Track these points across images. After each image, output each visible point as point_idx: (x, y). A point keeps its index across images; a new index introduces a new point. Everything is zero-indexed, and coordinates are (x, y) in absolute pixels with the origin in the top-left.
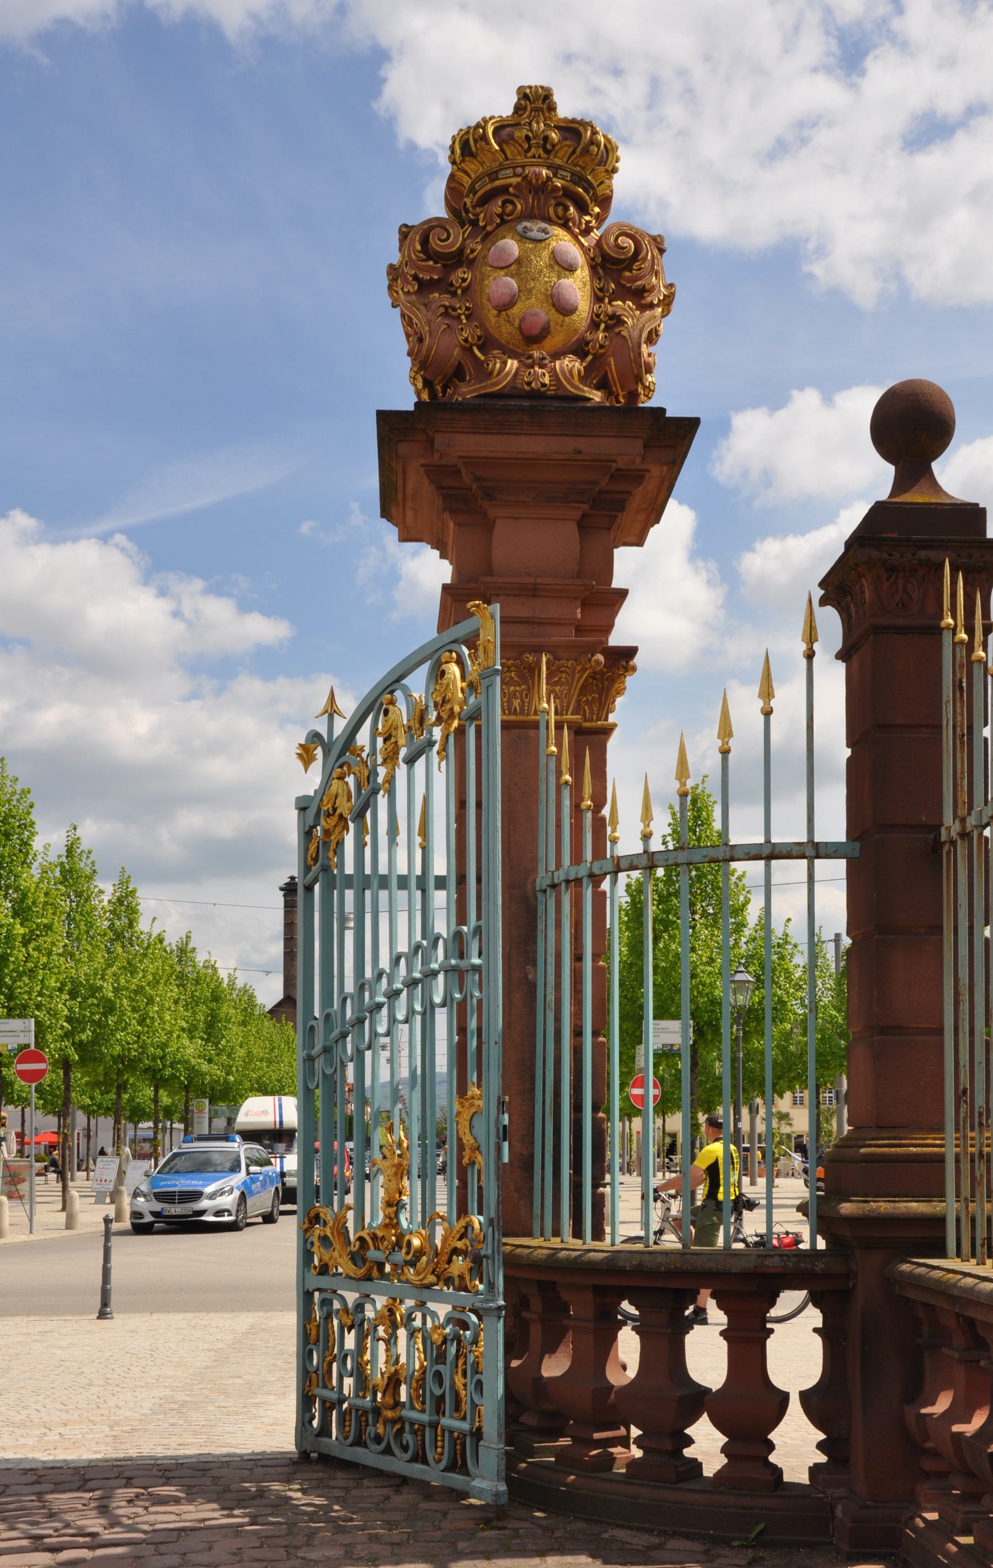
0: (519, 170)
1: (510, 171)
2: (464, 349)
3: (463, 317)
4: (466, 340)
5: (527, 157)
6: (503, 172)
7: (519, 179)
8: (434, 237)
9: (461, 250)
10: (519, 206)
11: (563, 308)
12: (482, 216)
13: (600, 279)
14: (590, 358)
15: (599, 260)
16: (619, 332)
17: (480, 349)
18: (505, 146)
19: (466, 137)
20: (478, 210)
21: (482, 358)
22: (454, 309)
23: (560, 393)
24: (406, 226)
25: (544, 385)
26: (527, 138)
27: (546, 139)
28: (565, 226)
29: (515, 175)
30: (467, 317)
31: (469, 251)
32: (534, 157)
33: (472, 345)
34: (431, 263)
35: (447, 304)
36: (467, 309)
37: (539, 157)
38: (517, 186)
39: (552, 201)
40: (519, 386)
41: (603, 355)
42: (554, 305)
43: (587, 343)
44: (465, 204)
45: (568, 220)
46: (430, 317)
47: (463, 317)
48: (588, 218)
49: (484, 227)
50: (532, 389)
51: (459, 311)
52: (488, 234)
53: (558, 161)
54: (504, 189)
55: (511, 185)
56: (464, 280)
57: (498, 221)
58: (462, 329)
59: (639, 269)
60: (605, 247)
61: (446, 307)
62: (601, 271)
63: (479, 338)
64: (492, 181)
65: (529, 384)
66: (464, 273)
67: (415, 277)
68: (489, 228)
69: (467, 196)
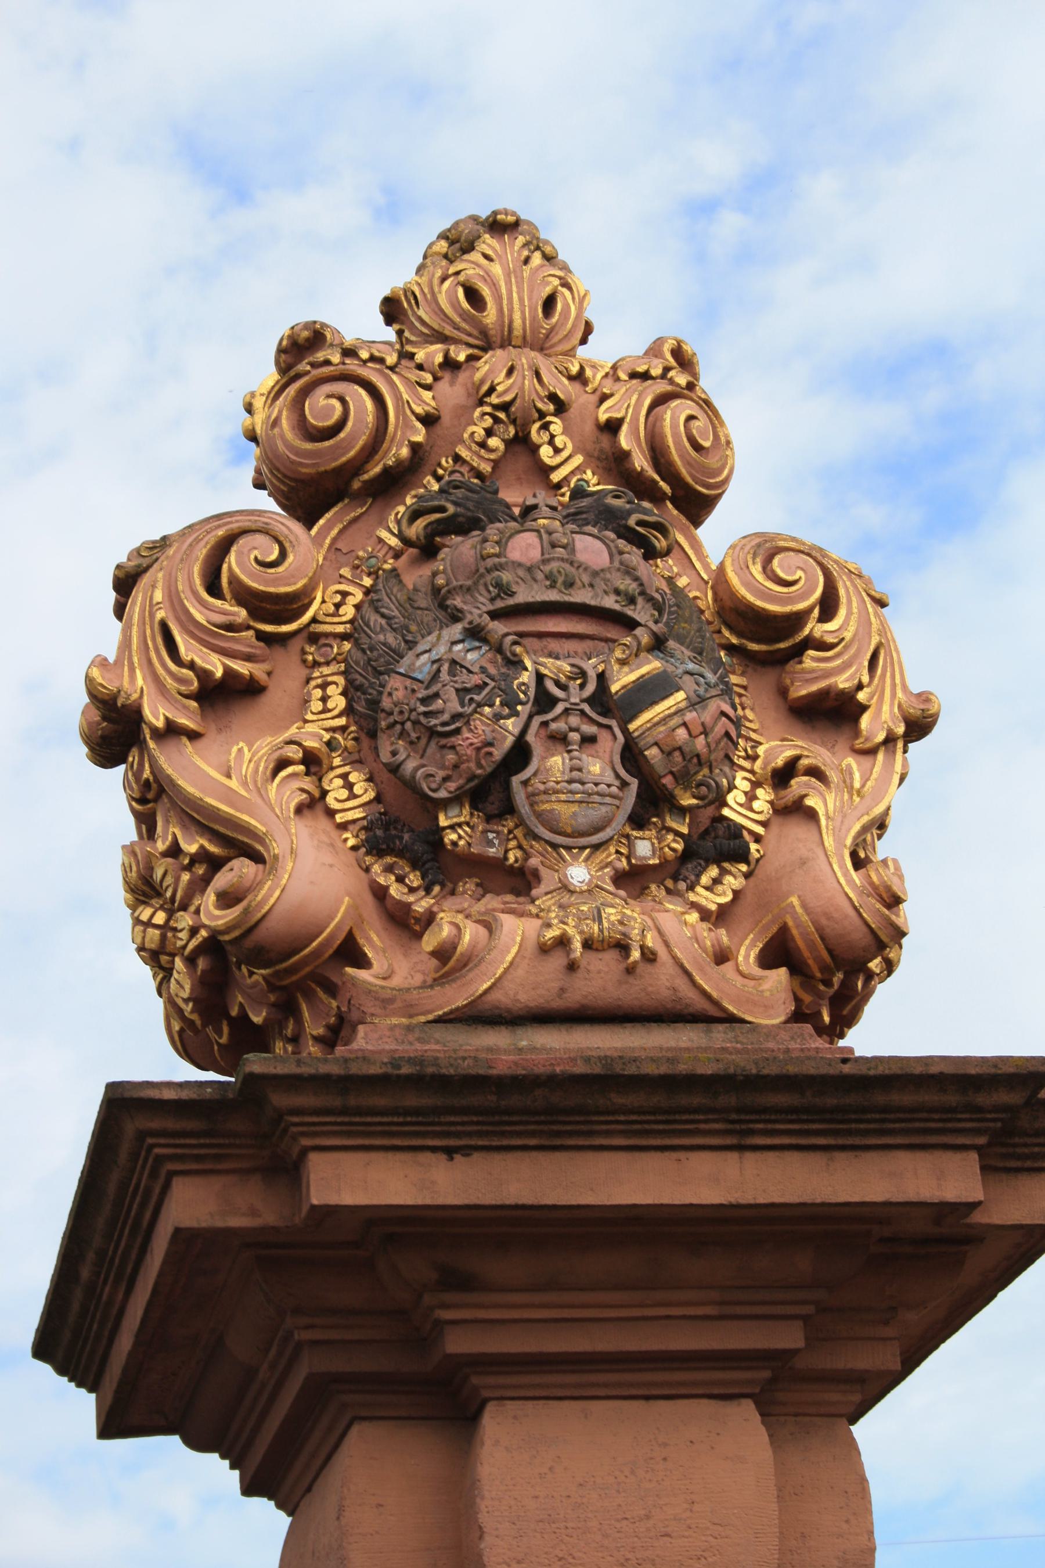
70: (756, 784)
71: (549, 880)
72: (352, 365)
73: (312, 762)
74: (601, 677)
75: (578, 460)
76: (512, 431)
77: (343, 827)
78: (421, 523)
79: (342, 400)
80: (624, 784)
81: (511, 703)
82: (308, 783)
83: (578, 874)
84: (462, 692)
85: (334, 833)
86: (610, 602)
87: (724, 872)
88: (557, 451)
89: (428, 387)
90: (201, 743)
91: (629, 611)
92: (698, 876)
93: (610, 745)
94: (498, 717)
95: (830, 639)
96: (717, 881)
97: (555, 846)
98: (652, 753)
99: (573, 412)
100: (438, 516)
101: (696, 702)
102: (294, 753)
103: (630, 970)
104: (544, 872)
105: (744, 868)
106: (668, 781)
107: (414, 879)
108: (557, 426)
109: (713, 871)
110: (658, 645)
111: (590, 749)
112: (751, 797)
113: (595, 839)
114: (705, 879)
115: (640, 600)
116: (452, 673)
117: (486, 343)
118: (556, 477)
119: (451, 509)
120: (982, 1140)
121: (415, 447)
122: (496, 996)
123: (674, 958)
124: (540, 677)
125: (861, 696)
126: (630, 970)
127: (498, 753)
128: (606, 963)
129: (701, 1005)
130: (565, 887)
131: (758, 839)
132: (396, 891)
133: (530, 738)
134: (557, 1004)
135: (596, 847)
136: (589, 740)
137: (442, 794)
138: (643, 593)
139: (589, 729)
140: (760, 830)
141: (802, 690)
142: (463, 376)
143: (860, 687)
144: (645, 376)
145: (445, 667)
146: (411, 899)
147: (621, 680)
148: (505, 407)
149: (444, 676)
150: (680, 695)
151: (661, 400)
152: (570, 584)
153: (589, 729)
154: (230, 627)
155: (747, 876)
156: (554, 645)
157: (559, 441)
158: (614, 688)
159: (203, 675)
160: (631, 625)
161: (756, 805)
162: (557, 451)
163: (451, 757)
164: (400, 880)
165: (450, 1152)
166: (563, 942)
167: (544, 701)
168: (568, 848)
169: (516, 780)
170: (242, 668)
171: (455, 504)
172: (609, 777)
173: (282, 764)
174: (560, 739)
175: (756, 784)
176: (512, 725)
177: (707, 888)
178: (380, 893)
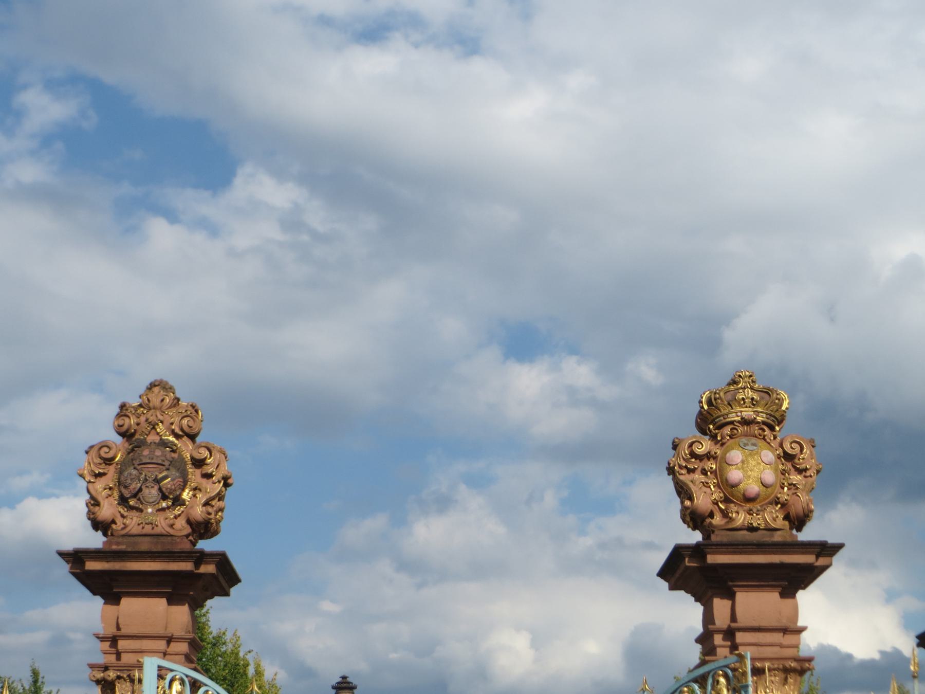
0: (739, 414)
1: (734, 415)
2: (714, 503)
3: (712, 487)
4: (715, 499)
5: (743, 408)
6: (730, 415)
7: (739, 419)
8: (695, 447)
9: (709, 452)
10: (740, 431)
11: (767, 484)
12: (719, 435)
13: (783, 464)
14: (779, 506)
15: (782, 454)
16: (796, 493)
17: (721, 502)
18: (731, 403)
19: (709, 395)
20: (717, 431)
21: (723, 507)
22: (707, 483)
23: (767, 528)
24: (677, 438)
25: (759, 524)
26: (743, 399)
27: (752, 399)
28: (764, 439)
29: (738, 416)
30: (714, 487)
31: (713, 453)
32: (746, 407)
33: (717, 502)
34: (693, 460)
35: (703, 481)
36: (714, 483)
37: (750, 407)
38: (739, 422)
39: (757, 428)
40: (746, 525)
41: (787, 504)
42: (762, 483)
43: (778, 498)
44: (709, 428)
45: (764, 436)
46: (696, 489)
47: (712, 487)
48: (774, 433)
49: (721, 440)
50: (753, 526)
51: (710, 484)
52: (722, 445)
53: (760, 410)
54: (732, 423)
55: (735, 421)
56: (712, 468)
57: (728, 438)
58: (712, 494)
59: (803, 459)
60: (785, 449)
61: (703, 483)
62: (783, 460)
63: (721, 498)
64: (724, 419)
65: (752, 524)
66: (711, 464)
67: (686, 467)
68: (724, 441)
69: (710, 424)
70: (190, 491)
71: (145, 511)
72: (127, 413)
73: (110, 489)
74: (156, 476)
75: (165, 431)
76: (152, 426)
77: (115, 500)
78: (131, 446)
79: (124, 420)
80: (159, 495)
81: (139, 480)
82: (110, 493)
83: (150, 510)
84: (131, 479)
85: (113, 501)
86: (160, 462)
87: (181, 507)
88: (161, 429)
89: (139, 418)
90: (94, 484)
91: (164, 463)
92: (175, 509)
93: (156, 487)
94: (137, 483)
95: (208, 463)
96: (179, 509)
97: (147, 505)
98: (164, 489)
99: (165, 423)
100: (133, 445)
101: (172, 480)
102: (107, 487)
103: (153, 528)
104: (144, 510)
105: (185, 506)
106: (167, 494)
107: (126, 510)
108: (160, 424)
109: (179, 507)
110: (168, 469)
111: (153, 489)
112: (188, 493)
113: (154, 504)
114: (177, 509)
115: (166, 461)
116: (130, 476)
117: (149, 409)
118: (160, 434)
119: (136, 444)
120: (194, 560)
121: (135, 430)
122: (130, 532)
123: (162, 526)
124: (146, 475)
125: (214, 473)
126: (153, 528)
127: (137, 490)
128: (150, 527)
129: (165, 533)
130: (147, 513)
131: (189, 501)
132: (122, 511)
133: (142, 487)
134: (141, 533)
135: (154, 505)
136: (153, 487)
137: (128, 496)
138: (167, 459)
139: (153, 485)
140: (189, 500)
141: (204, 472)
142: (145, 415)
143: (213, 472)
144: (181, 412)
145: (129, 475)
146: (124, 513)
147: (161, 476)
148: (150, 422)
149: (129, 476)
150: (170, 479)
151: (183, 418)
152: (152, 459)
153: (153, 485)
154: (100, 464)
155: (185, 508)
156: (151, 470)
157: (161, 428)
158: (158, 478)
159: (95, 473)
160: (164, 465)
161: (189, 495)
162: (161, 429)
163: (129, 490)
164: (123, 509)
165: (108, 562)
166: (142, 523)
167: (146, 480)
168: (149, 505)
169: (140, 494)
170: (101, 471)
171: (137, 443)
172: (156, 493)
173: (105, 489)
174: (147, 487)
175: (190, 491)
176: (139, 485)
177: (177, 510)
178: (120, 512)
